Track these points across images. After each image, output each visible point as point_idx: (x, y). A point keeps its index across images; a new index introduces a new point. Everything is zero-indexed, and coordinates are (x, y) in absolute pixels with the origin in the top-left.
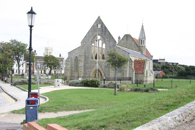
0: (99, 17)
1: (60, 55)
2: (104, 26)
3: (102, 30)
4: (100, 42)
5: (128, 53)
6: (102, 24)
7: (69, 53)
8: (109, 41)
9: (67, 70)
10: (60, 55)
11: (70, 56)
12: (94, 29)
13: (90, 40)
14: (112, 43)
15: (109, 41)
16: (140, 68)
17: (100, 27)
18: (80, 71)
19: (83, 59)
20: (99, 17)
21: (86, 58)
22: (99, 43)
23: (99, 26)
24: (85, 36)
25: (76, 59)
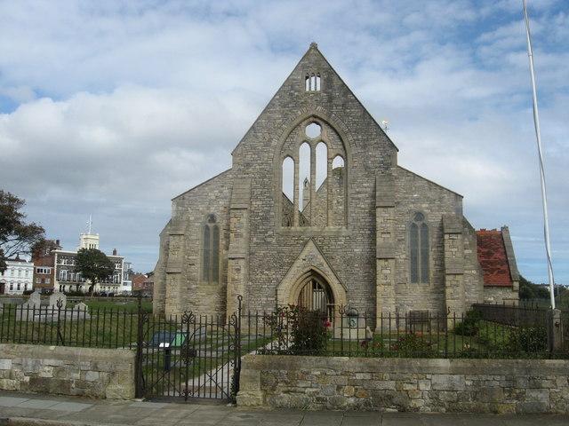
0: (314, 46)
1: (115, 253)
2: (336, 83)
3: (330, 99)
4: (321, 150)
5: (452, 196)
6: (329, 75)
7: (180, 200)
8: (364, 147)
9: (169, 277)
10: (115, 253)
11: (182, 214)
12: (289, 95)
13: (274, 143)
14: (376, 155)
15: (364, 147)
16: (491, 263)
17: (319, 89)
18: (233, 280)
19: (242, 222)
20: (314, 46)
21: (259, 224)
22: (313, 155)
23: (315, 84)
24: (253, 127)
25: (211, 225)
